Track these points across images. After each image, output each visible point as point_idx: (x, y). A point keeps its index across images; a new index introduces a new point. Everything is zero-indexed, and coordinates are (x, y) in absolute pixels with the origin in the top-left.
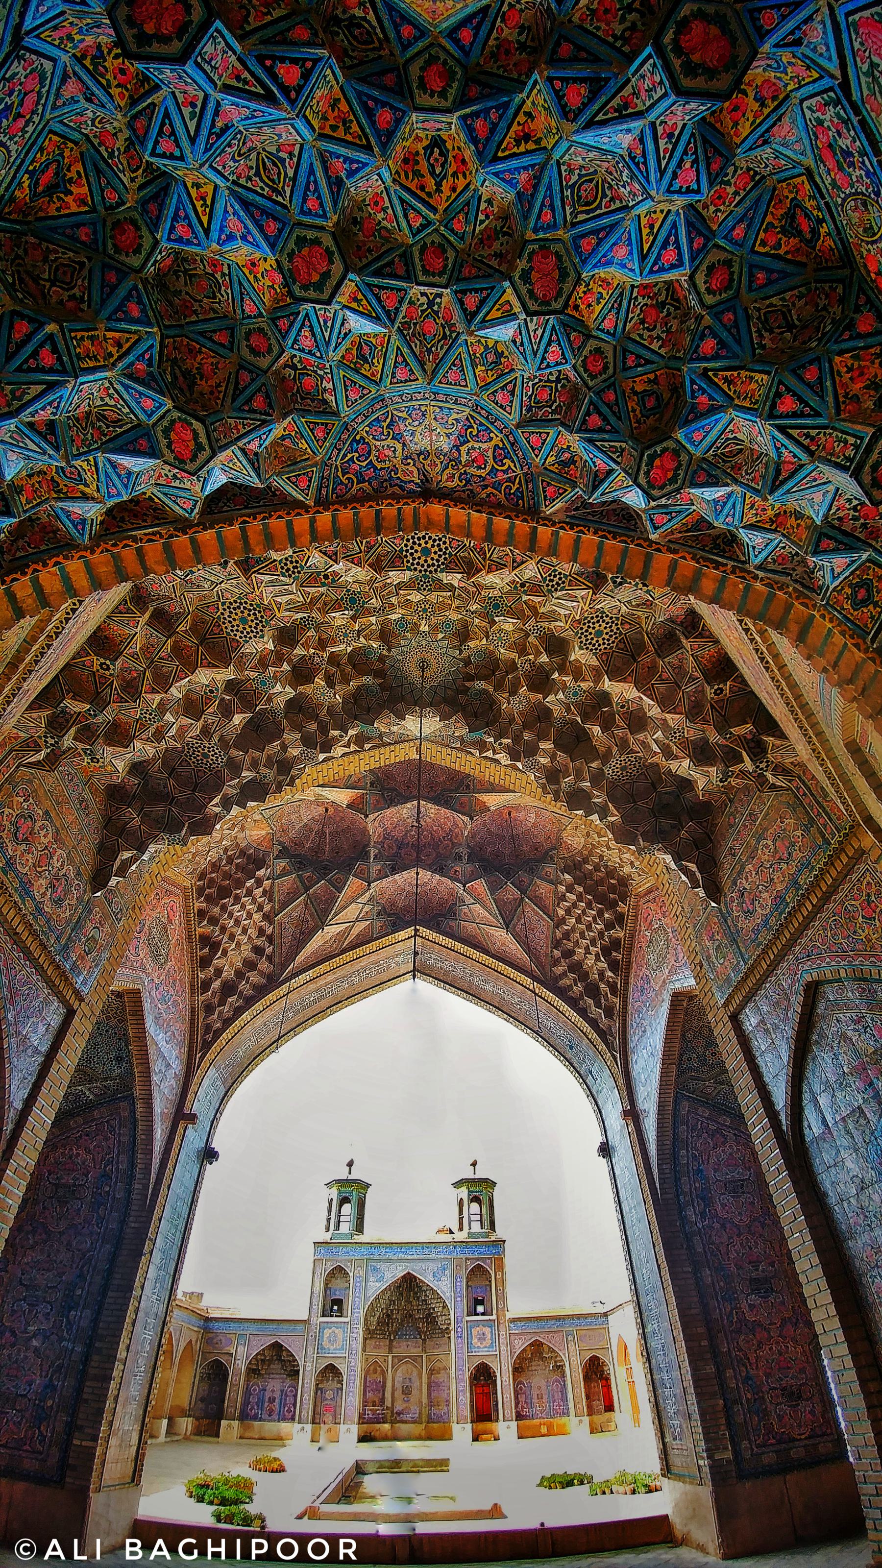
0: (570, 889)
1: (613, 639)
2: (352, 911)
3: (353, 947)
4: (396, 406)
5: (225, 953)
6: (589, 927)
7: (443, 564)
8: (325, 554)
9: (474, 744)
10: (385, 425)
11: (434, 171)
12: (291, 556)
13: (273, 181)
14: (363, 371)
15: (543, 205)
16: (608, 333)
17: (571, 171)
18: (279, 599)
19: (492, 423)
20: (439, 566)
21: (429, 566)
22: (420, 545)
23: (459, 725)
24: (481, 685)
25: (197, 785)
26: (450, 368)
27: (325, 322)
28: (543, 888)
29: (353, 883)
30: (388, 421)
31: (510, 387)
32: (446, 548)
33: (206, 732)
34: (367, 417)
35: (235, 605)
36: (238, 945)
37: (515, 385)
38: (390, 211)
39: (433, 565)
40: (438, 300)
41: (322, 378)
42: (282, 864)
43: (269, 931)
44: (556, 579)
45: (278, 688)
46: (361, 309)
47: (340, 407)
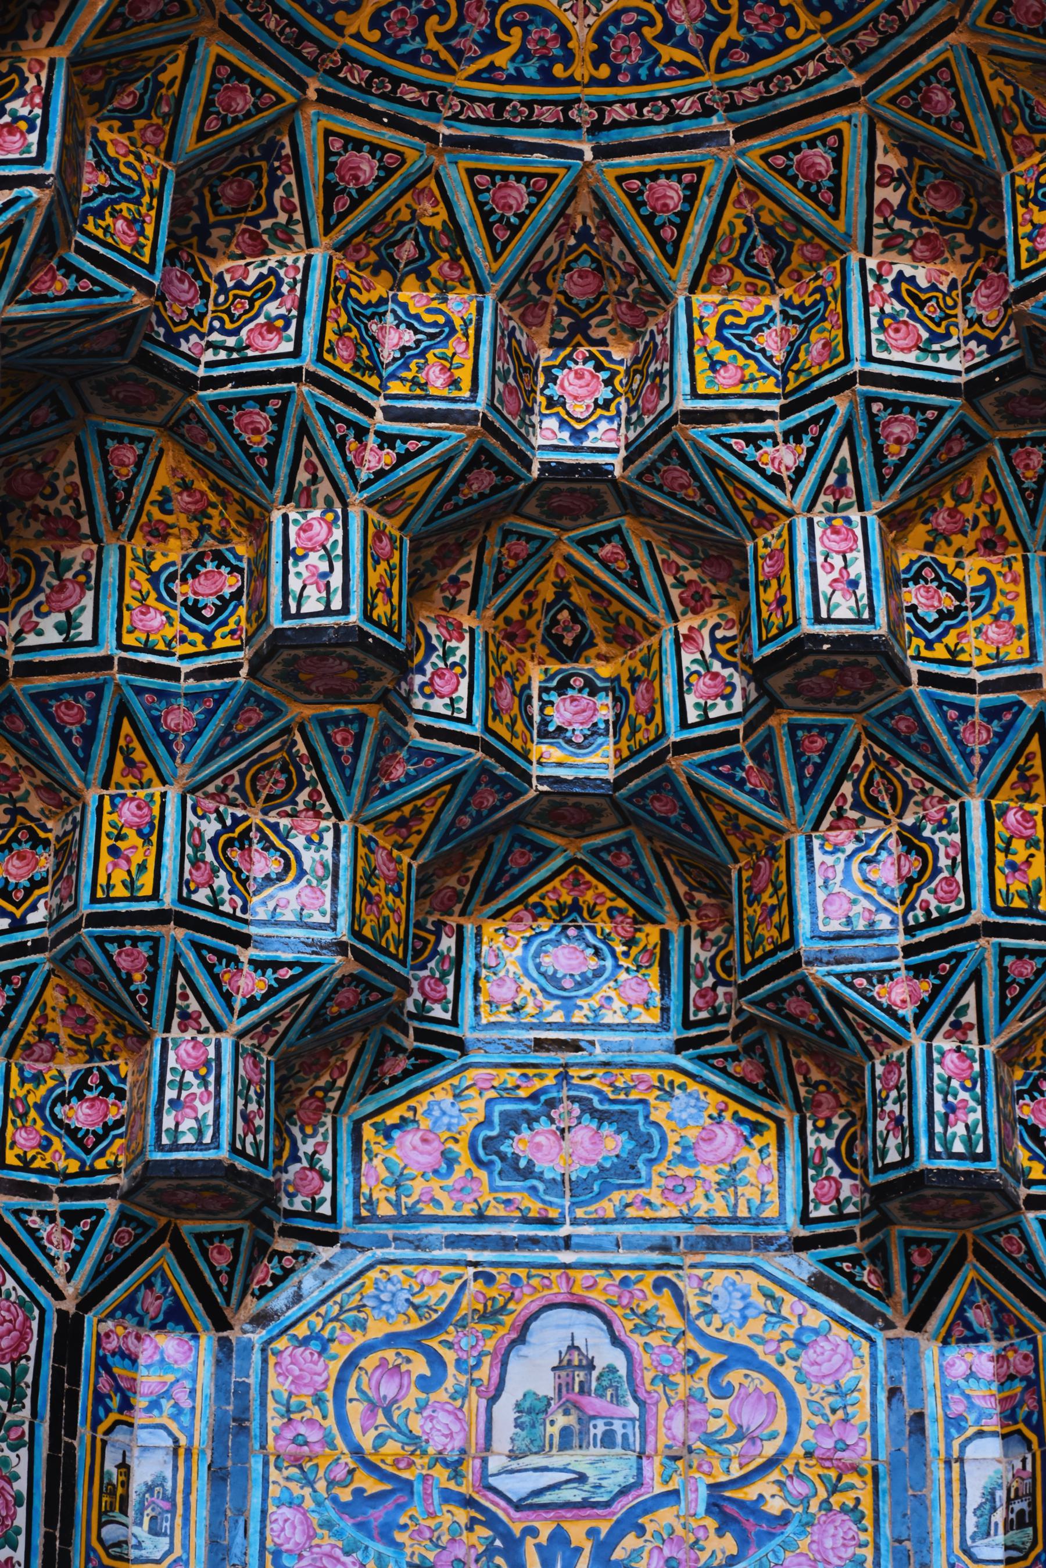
4: (696, 83)
10: (731, 32)
11: (572, 613)
13: (883, 776)
14: (778, 211)
15: (356, 755)
16: (119, 437)
17: (312, 807)
19: (379, 72)
26: (523, 217)
27: (841, 480)
30: (721, 42)
31: (341, 205)
34: (788, 70)
37: (327, 212)
38: (669, 580)
40: (560, 336)
41: (902, 212)
46: (750, 495)
47: (863, 132)
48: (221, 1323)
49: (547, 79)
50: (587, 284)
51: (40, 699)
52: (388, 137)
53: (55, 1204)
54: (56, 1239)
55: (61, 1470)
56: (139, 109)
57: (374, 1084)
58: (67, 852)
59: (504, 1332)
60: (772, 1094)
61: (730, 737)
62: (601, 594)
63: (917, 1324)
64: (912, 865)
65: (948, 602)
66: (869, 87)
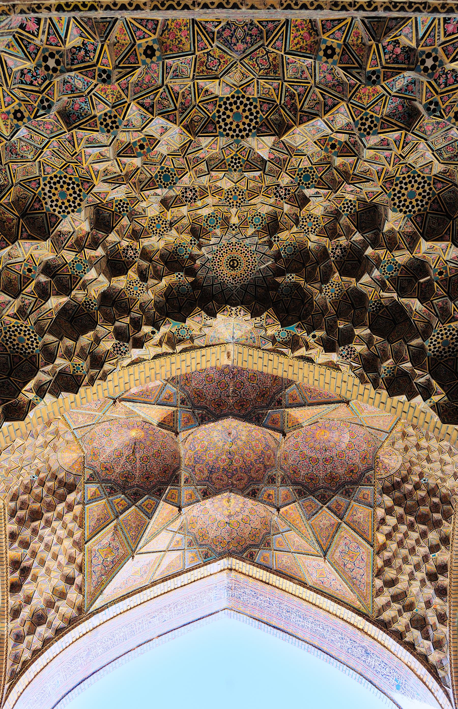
0: (389, 511)
1: (426, 200)
2: (163, 540)
3: (164, 580)
5: (35, 578)
6: (412, 551)
7: (254, 128)
8: (142, 105)
9: (285, 344)
12: (110, 111)
18: (96, 166)
20: (250, 131)
21: (240, 131)
22: (231, 110)
23: (270, 321)
24: (292, 278)
25: (12, 371)
28: (360, 513)
29: (164, 510)
32: (257, 113)
33: (22, 313)
35: (55, 180)
36: (48, 571)
39: (245, 129)
42: (92, 488)
43: (79, 560)
44: (368, 123)
45: (92, 274)
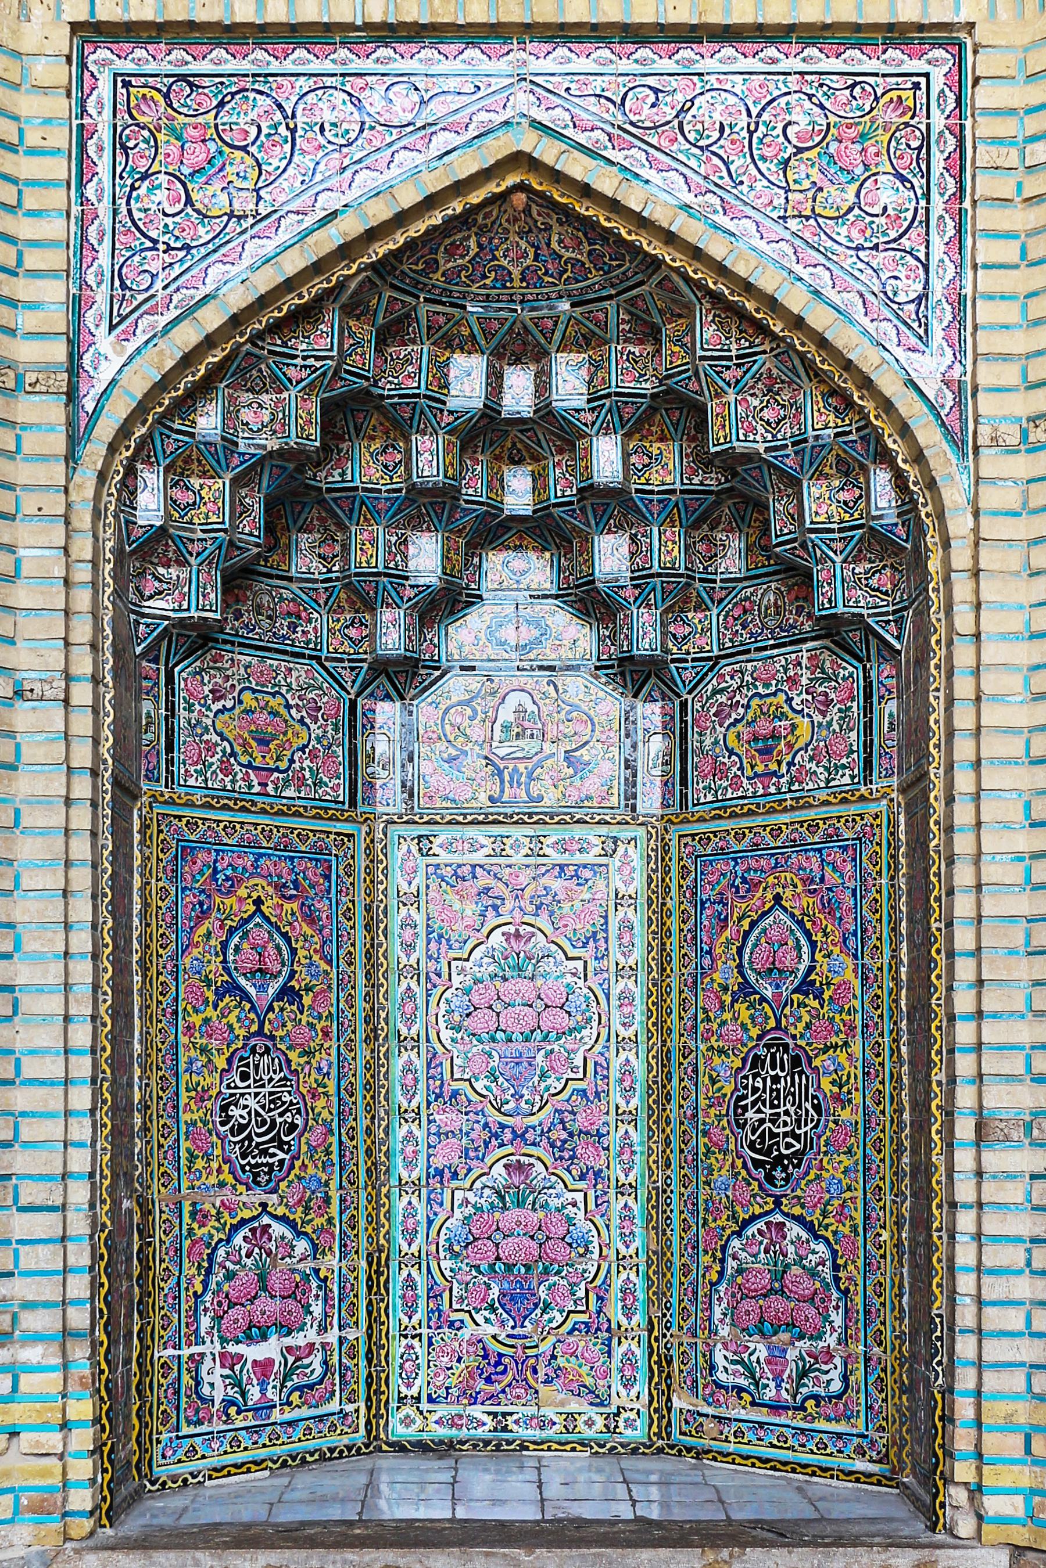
48: (402, 698)
49: (504, 287)
50: (519, 346)
51: (335, 500)
52: (449, 310)
53: (346, 664)
54: (347, 676)
55: (353, 752)
56: (362, 314)
57: (452, 613)
58: (346, 548)
59: (497, 700)
60: (588, 615)
61: (571, 503)
62: (528, 447)
63: (635, 696)
64: (634, 548)
65: (646, 460)
66: (618, 294)
